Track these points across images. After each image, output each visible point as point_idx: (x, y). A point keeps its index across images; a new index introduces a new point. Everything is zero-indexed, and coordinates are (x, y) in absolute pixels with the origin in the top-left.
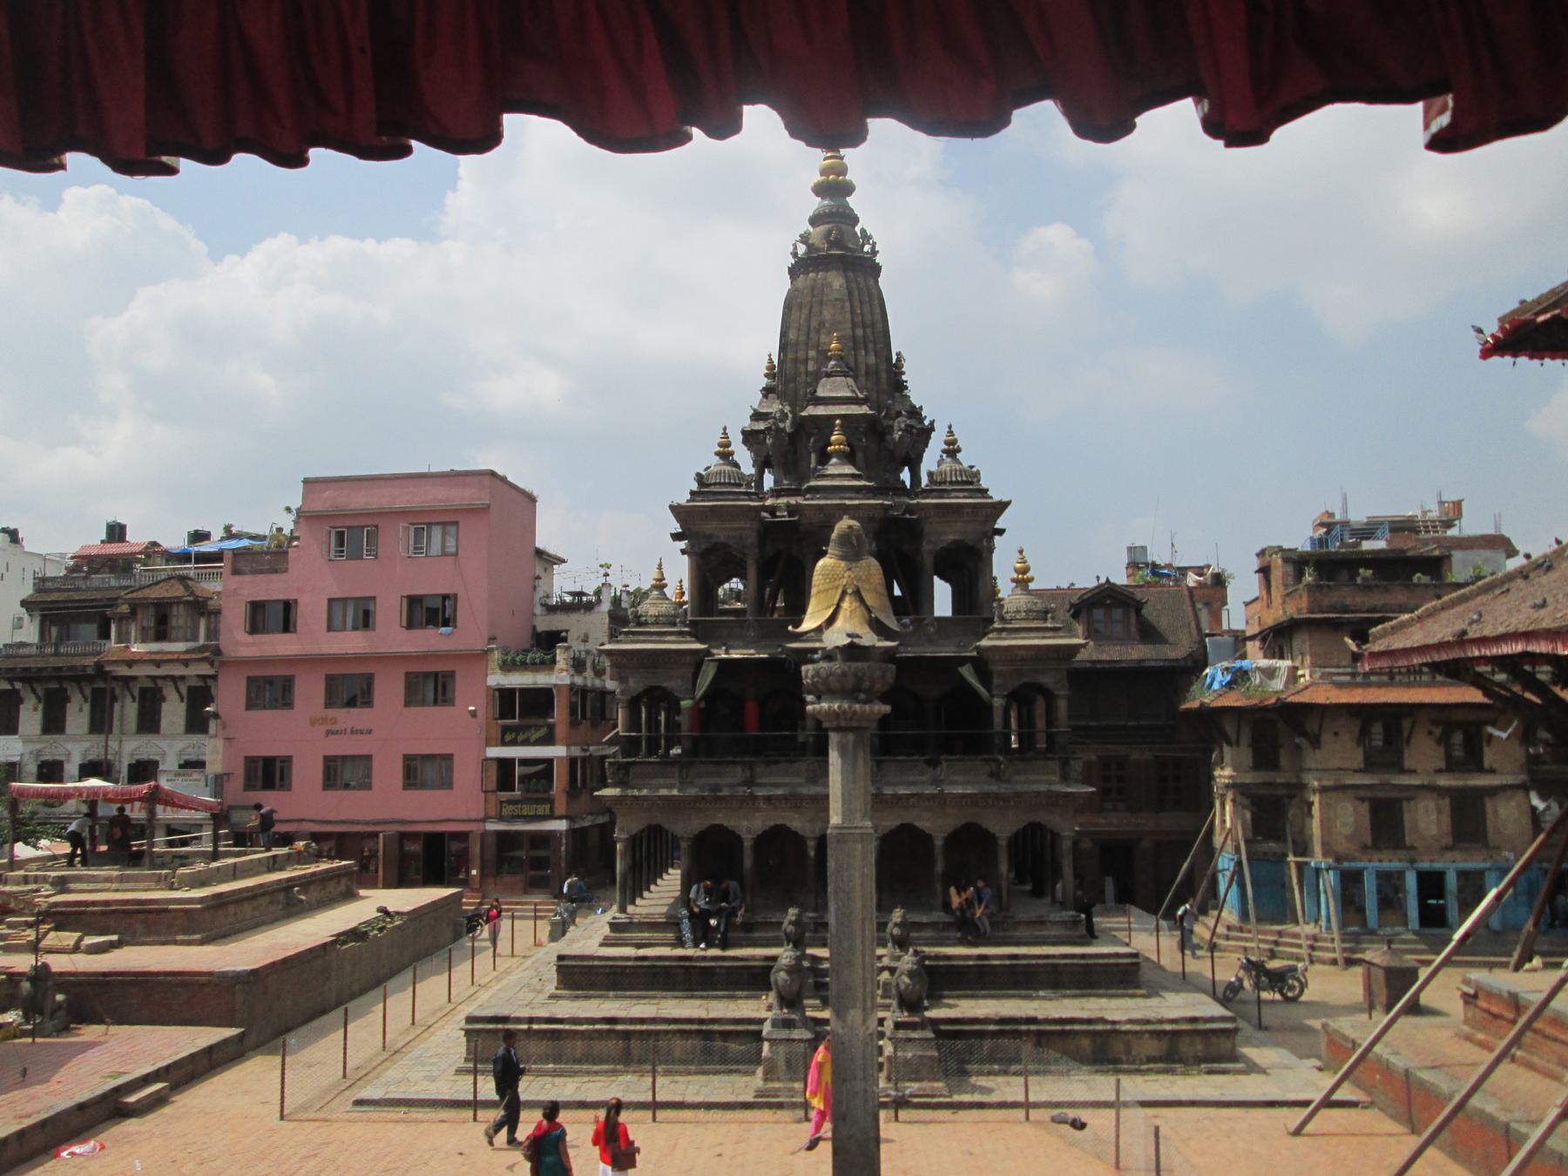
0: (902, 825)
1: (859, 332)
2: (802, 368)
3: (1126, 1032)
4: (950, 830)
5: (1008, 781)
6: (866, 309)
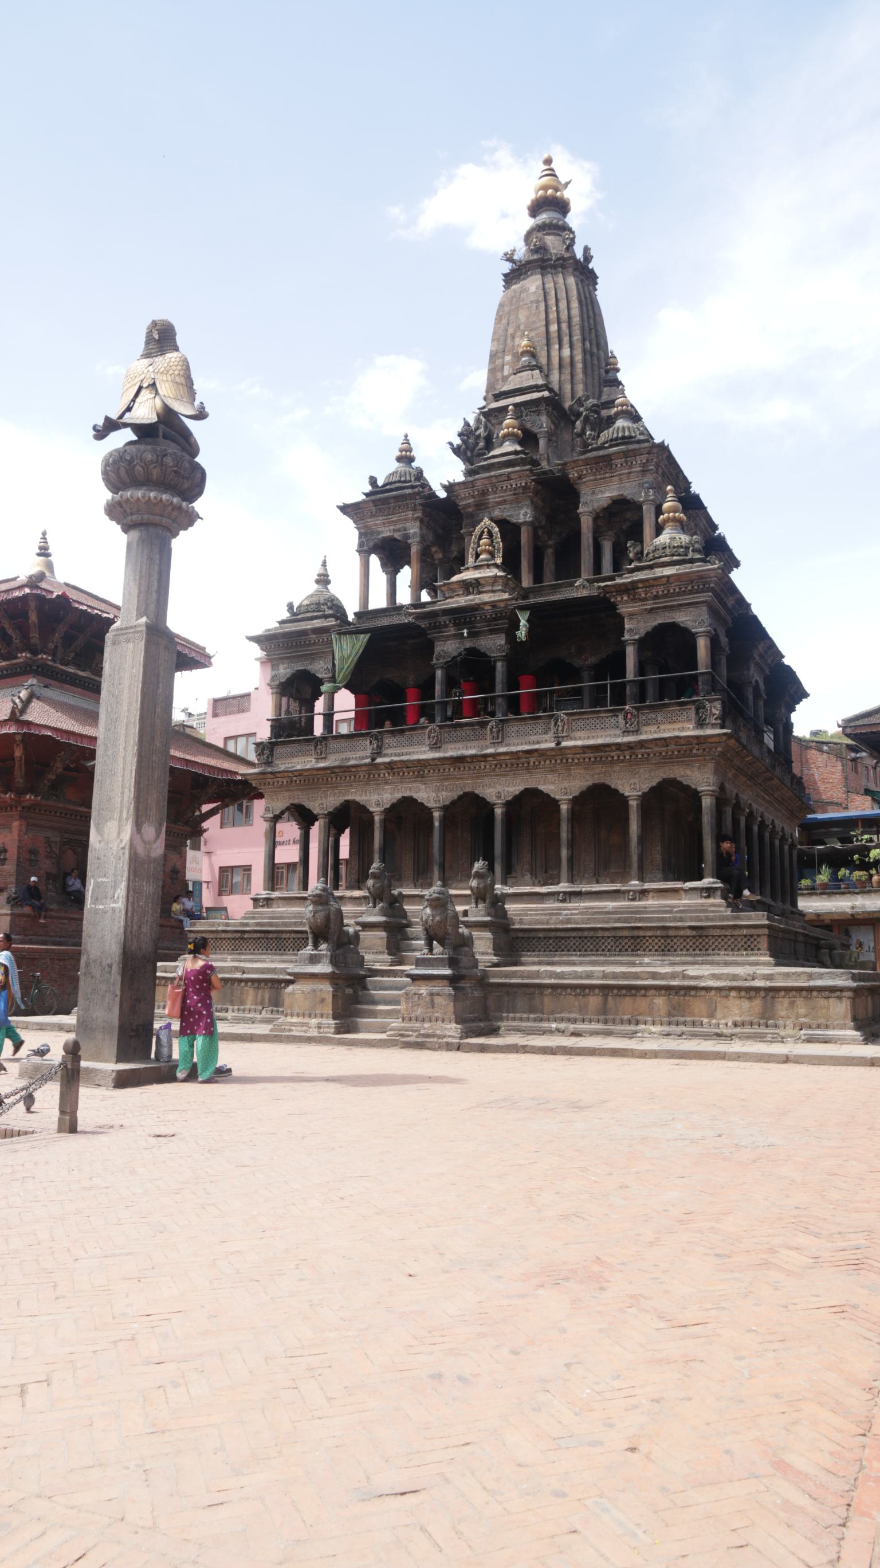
0: (526, 789)
1: (554, 328)
2: (499, 375)
3: (707, 989)
4: (576, 793)
5: (637, 732)
6: (563, 305)
